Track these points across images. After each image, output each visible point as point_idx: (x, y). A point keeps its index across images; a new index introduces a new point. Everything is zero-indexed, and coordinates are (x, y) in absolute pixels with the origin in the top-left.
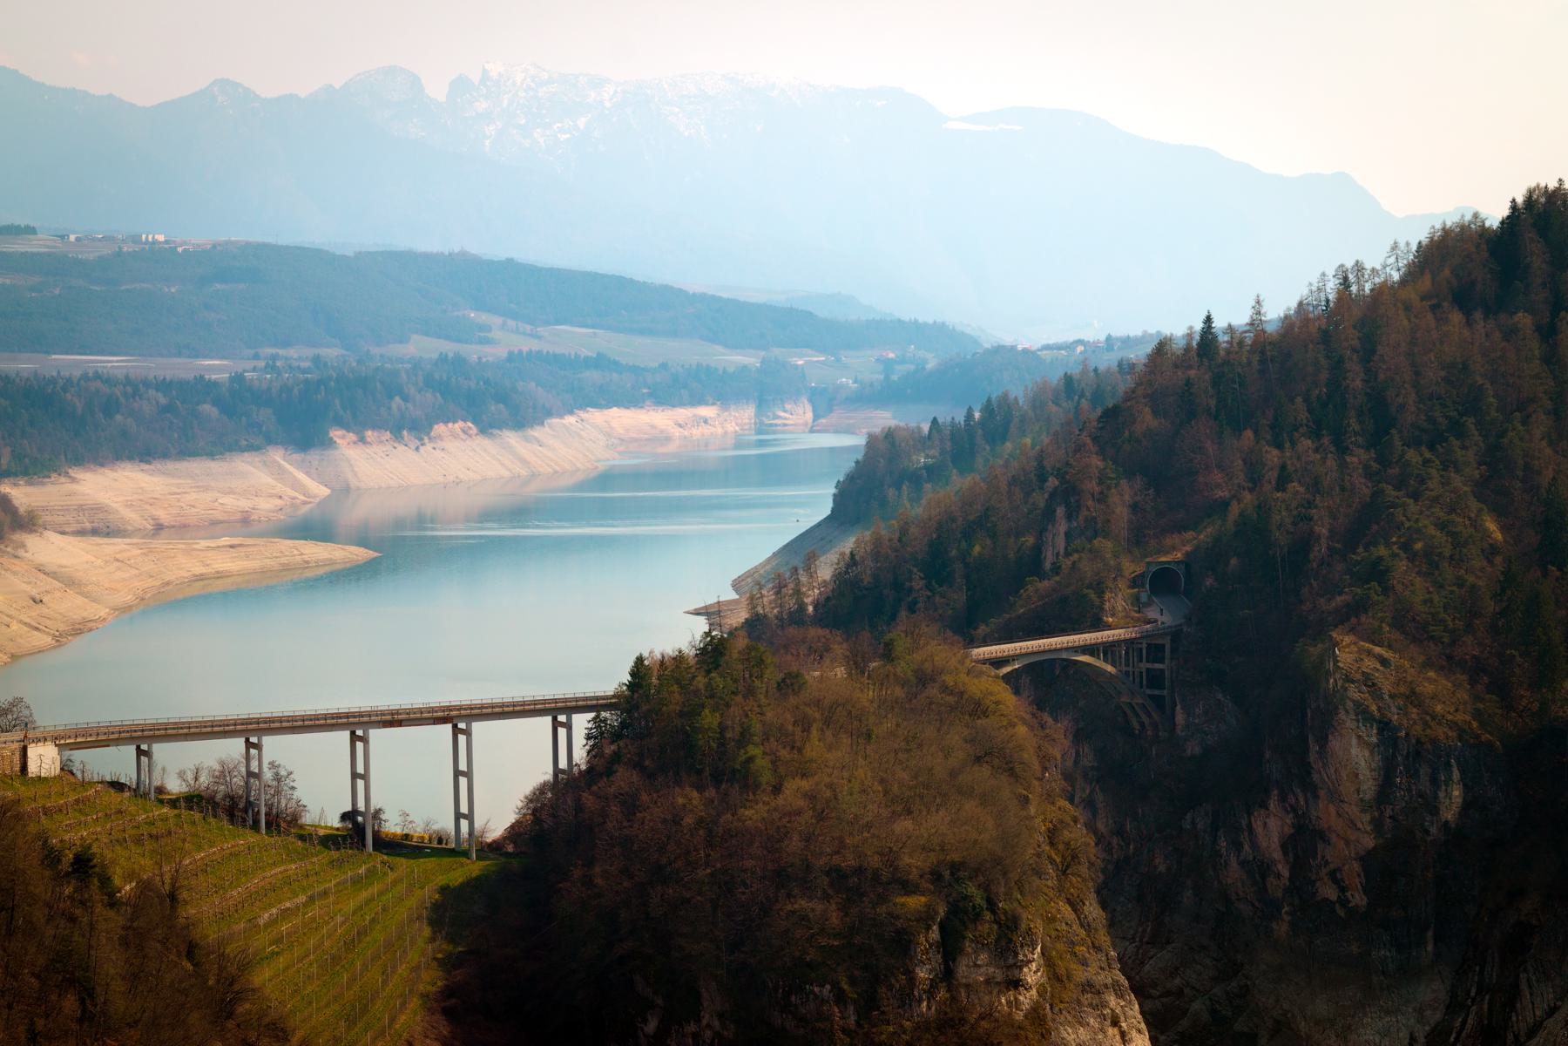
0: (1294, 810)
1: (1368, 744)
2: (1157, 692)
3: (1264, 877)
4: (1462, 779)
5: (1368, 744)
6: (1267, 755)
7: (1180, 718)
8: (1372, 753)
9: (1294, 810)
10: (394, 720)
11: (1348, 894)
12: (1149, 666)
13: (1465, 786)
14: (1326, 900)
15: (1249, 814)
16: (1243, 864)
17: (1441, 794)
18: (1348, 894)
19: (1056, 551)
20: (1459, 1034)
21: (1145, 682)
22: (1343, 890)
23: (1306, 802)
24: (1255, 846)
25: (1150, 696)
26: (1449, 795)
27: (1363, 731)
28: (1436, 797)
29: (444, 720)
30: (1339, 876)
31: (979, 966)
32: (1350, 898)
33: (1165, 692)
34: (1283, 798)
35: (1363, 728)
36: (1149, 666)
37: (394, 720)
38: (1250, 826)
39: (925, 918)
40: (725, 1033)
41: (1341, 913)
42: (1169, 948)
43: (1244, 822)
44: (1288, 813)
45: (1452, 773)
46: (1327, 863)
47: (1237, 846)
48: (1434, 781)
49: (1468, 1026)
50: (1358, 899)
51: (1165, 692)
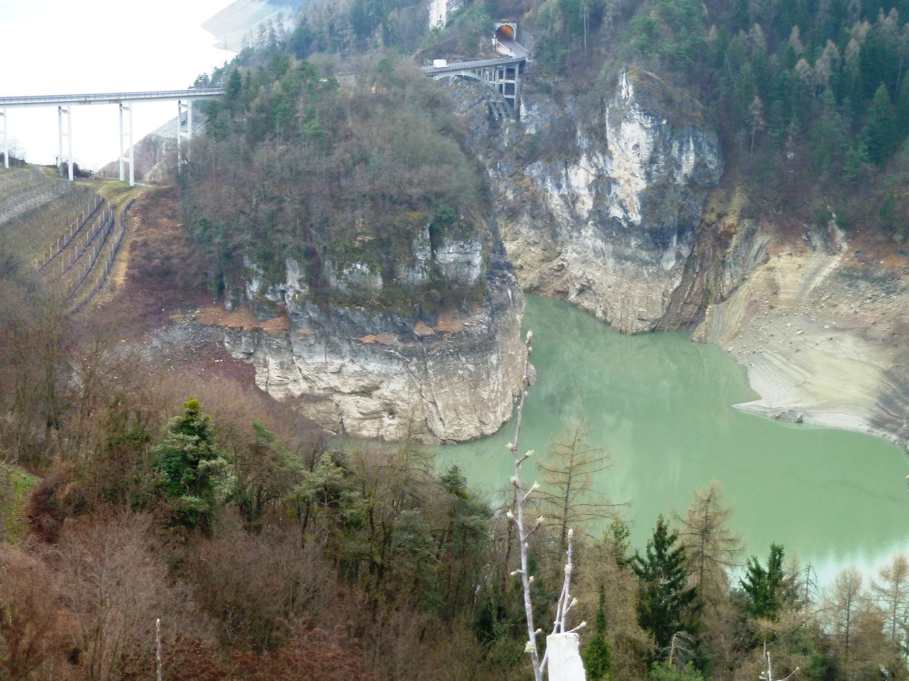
0: (596, 166)
1: (646, 129)
2: (509, 97)
3: (574, 203)
4: (694, 150)
5: (646, 129)
6: (579, 133)
7: (523, 111)
8: (648, 133)
9: (596, 166)
10: (86, 100)
11: (630, 214)
12: (507, 81)
13: (696, 154)
14: (614, 218)
15: (566, 168)
16: (562, 196)
17: (684, 158)
18: (630, 214)
19: (439, 14)
20: (689, 294)
21: (504, 91)
22: (626, 211)
23: (605, 161)
24: (569, 186)
25: (507, 99)
26: (687, 159)
27: (643, 121)
28: (681, 160)
29: (116, 101)
30: (624, 204)
31: (450, 253)
32: (630, 216)
33: (514, 97)
34: (590, 159)
35: (644, 120)
36: (507, 81)
37: (86, 100)
38: (567, 174)
39: (421, 224)
40: (303, 290)
41: (625, 225)
42: (515, 243)
43: (563, 172)
44: (592, 167)
45: (689, 146)
46: (617, 196)
47: (559, 187)
48: (680, 151)
49: (695, 289)
50: (636, 218)
51: (514, 97)
